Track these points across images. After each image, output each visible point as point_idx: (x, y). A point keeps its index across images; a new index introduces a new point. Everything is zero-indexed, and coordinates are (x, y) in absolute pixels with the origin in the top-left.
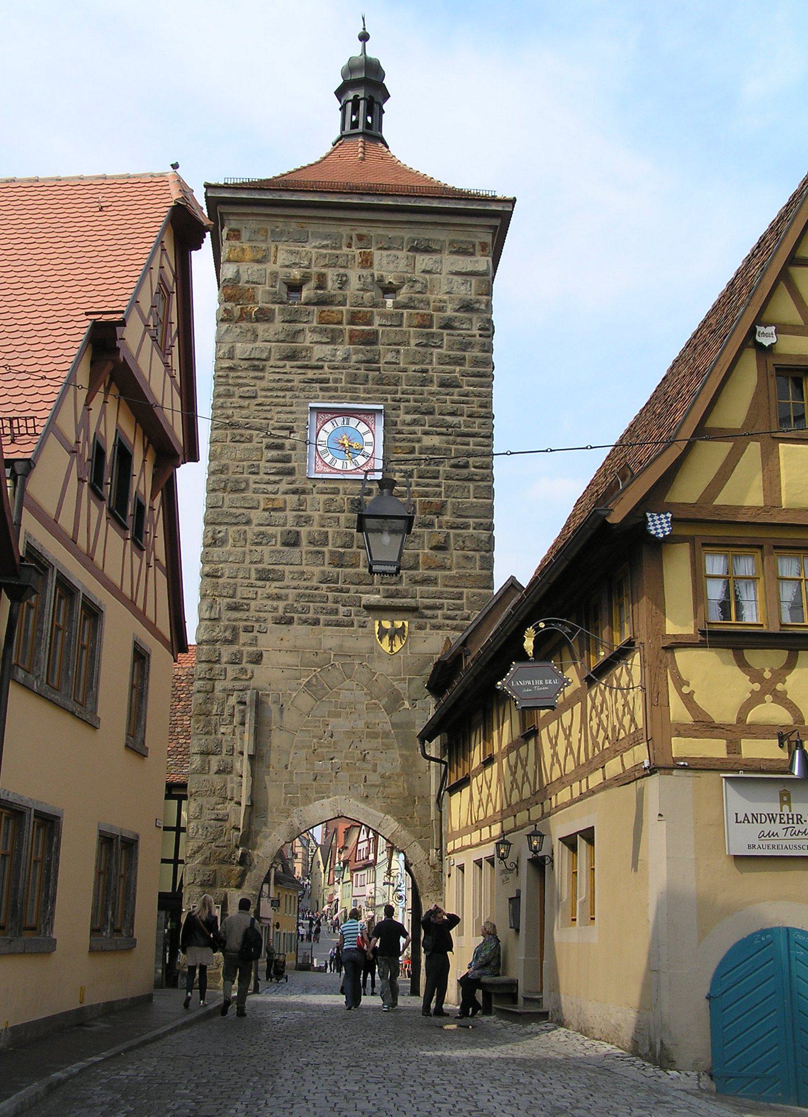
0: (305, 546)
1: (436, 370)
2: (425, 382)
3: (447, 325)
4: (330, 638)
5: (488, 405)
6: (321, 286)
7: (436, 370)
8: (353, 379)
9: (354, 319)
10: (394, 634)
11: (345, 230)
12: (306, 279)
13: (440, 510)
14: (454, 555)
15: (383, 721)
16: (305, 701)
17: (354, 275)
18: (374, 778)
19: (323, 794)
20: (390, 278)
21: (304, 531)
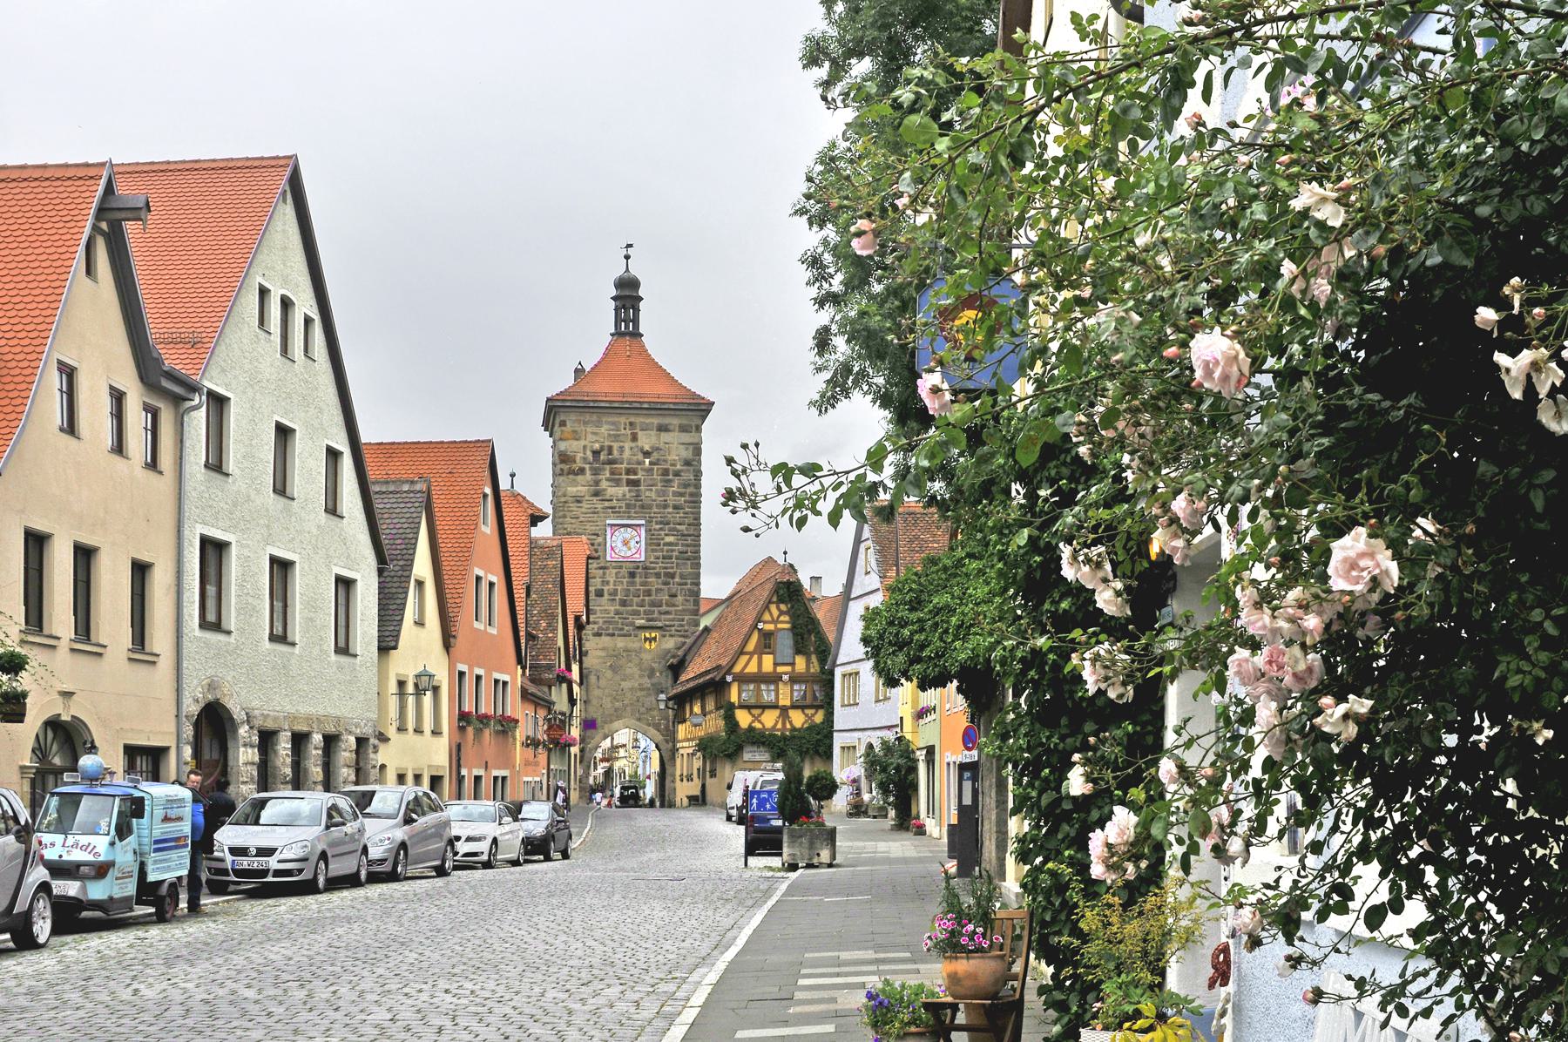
0: (606, 596)
1: (671, 500)
2: (665, 507)
3: (677, 474)
4: (621, 643)
5: (697, 519)
6: (610, 453)
7: (671, 500)
8: (628, 506)
9: (628, 472)
10: (651, 640)
11: (623, 420)
12: (602, 448)
13: (673, 576)
14: (680, 598)
15: (647, 682)
16: (609, 674)
17: (627, 445)
18: (643, 710)
19: (619, 718)
20: (647, 448)
21: (606, 588)
